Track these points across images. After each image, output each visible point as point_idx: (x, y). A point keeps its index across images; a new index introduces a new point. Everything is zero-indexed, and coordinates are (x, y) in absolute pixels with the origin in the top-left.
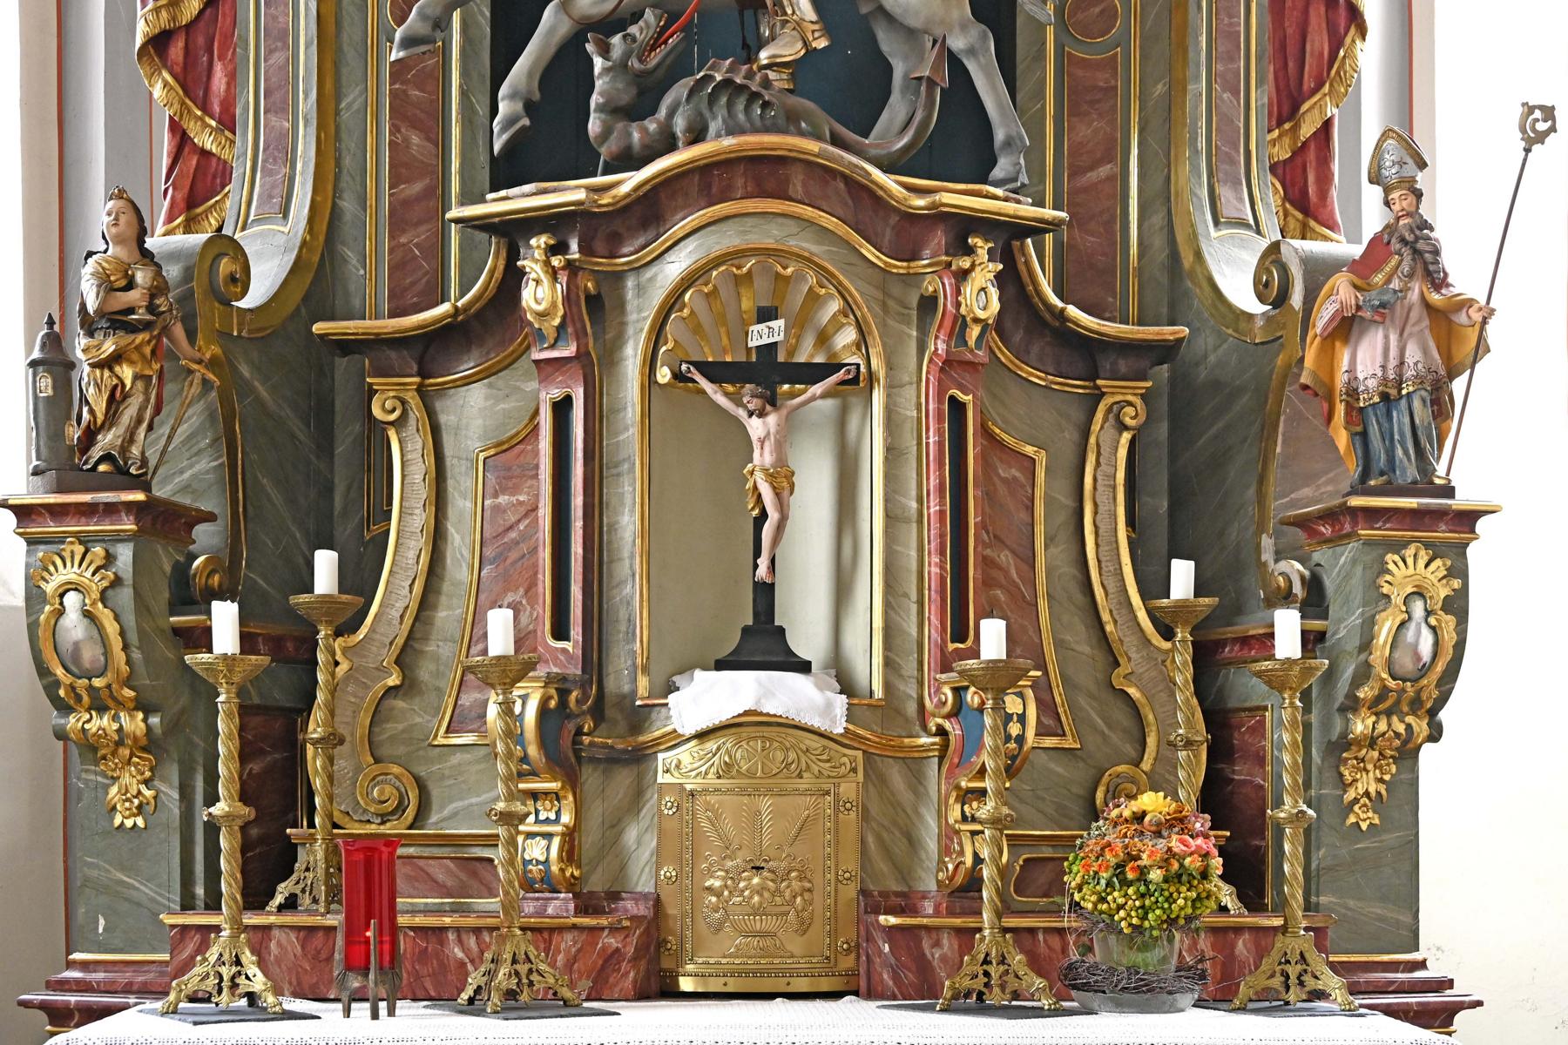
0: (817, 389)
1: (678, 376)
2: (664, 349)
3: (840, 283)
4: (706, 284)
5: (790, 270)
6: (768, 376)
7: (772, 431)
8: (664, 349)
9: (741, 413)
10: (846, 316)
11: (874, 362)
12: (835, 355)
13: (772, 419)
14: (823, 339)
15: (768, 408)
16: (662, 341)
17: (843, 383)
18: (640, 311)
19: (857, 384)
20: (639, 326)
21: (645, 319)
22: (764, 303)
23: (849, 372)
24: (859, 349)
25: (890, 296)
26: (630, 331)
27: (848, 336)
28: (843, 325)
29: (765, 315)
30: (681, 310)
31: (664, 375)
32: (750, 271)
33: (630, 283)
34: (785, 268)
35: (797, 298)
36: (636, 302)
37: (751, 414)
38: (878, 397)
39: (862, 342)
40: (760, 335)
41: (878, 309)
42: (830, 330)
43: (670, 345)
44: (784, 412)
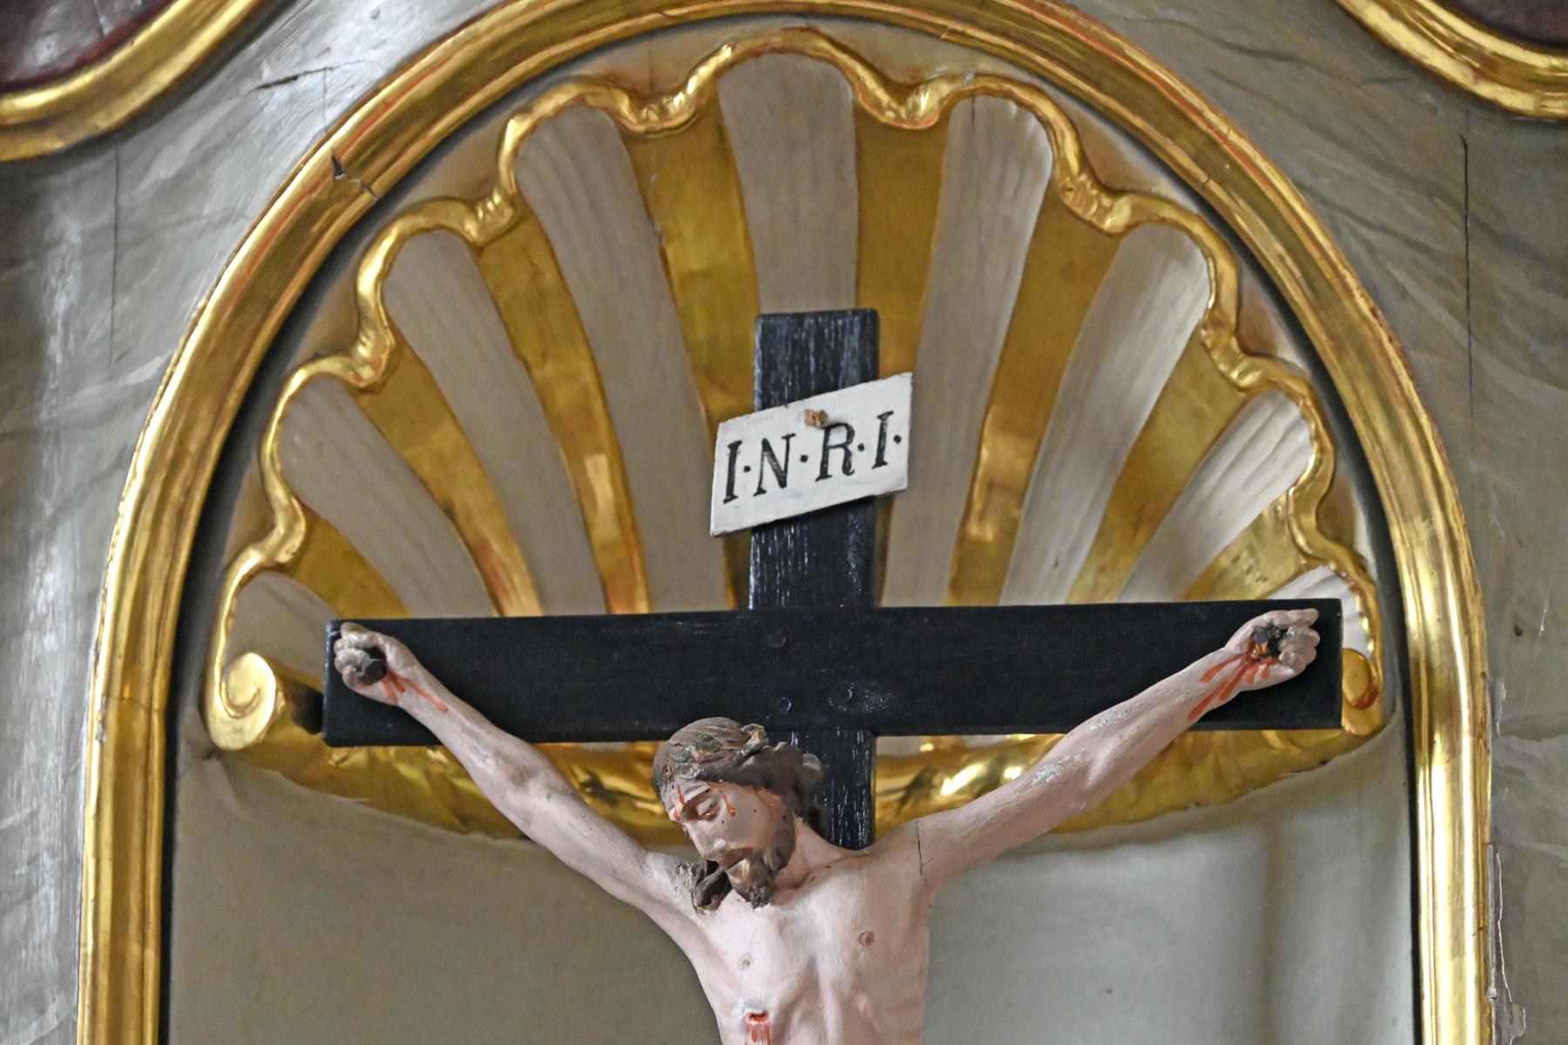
0: (1098, 742)
1: (329, 710)
2: (252, 559)
3: (1210, 150)
4: (473, 200)
5: (925, 101)
6: (824, 678)
7: (830, 969)
8: (252, 559)
9: (663, 883)
10: (1255, 348)
11: (1424, 605)
12: (1215, 576)
13: (829, 910)
14: (1147, 496)
15: (810, 846)
16: (238, 522)
17: (1245, 709)
18: (119, 357)
19: (1312, 703)
20: (109, 441)
21: (145, 395)
22: (808, 294)
23: (1272, 641)
24: (1343, 537)
25: (1504, 242)
26: (63, 468)
27: (1277, 461)
28: (1248, 400)
29: (808, 359)
30: (342, 345)
31: (246, 697)
32: (707, 109)
33: (71, 224)
34: (903, 90)
35: (988, 271)
36: (99, 323)
37: (713, 894)
38: (1447, 798)
39: (1350, 499)
40: (780, 465)
41: (1435, 310)
42: (1181, 442)
43: (286, 540)
44: (902, 868)
